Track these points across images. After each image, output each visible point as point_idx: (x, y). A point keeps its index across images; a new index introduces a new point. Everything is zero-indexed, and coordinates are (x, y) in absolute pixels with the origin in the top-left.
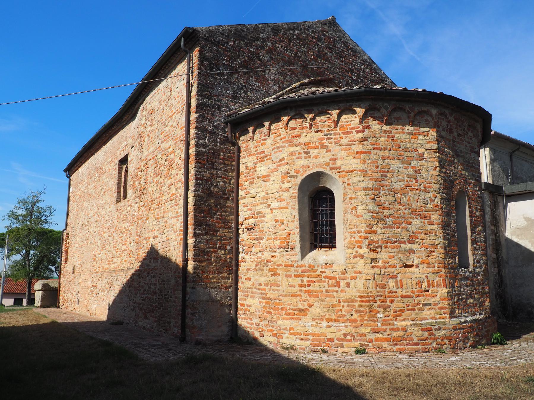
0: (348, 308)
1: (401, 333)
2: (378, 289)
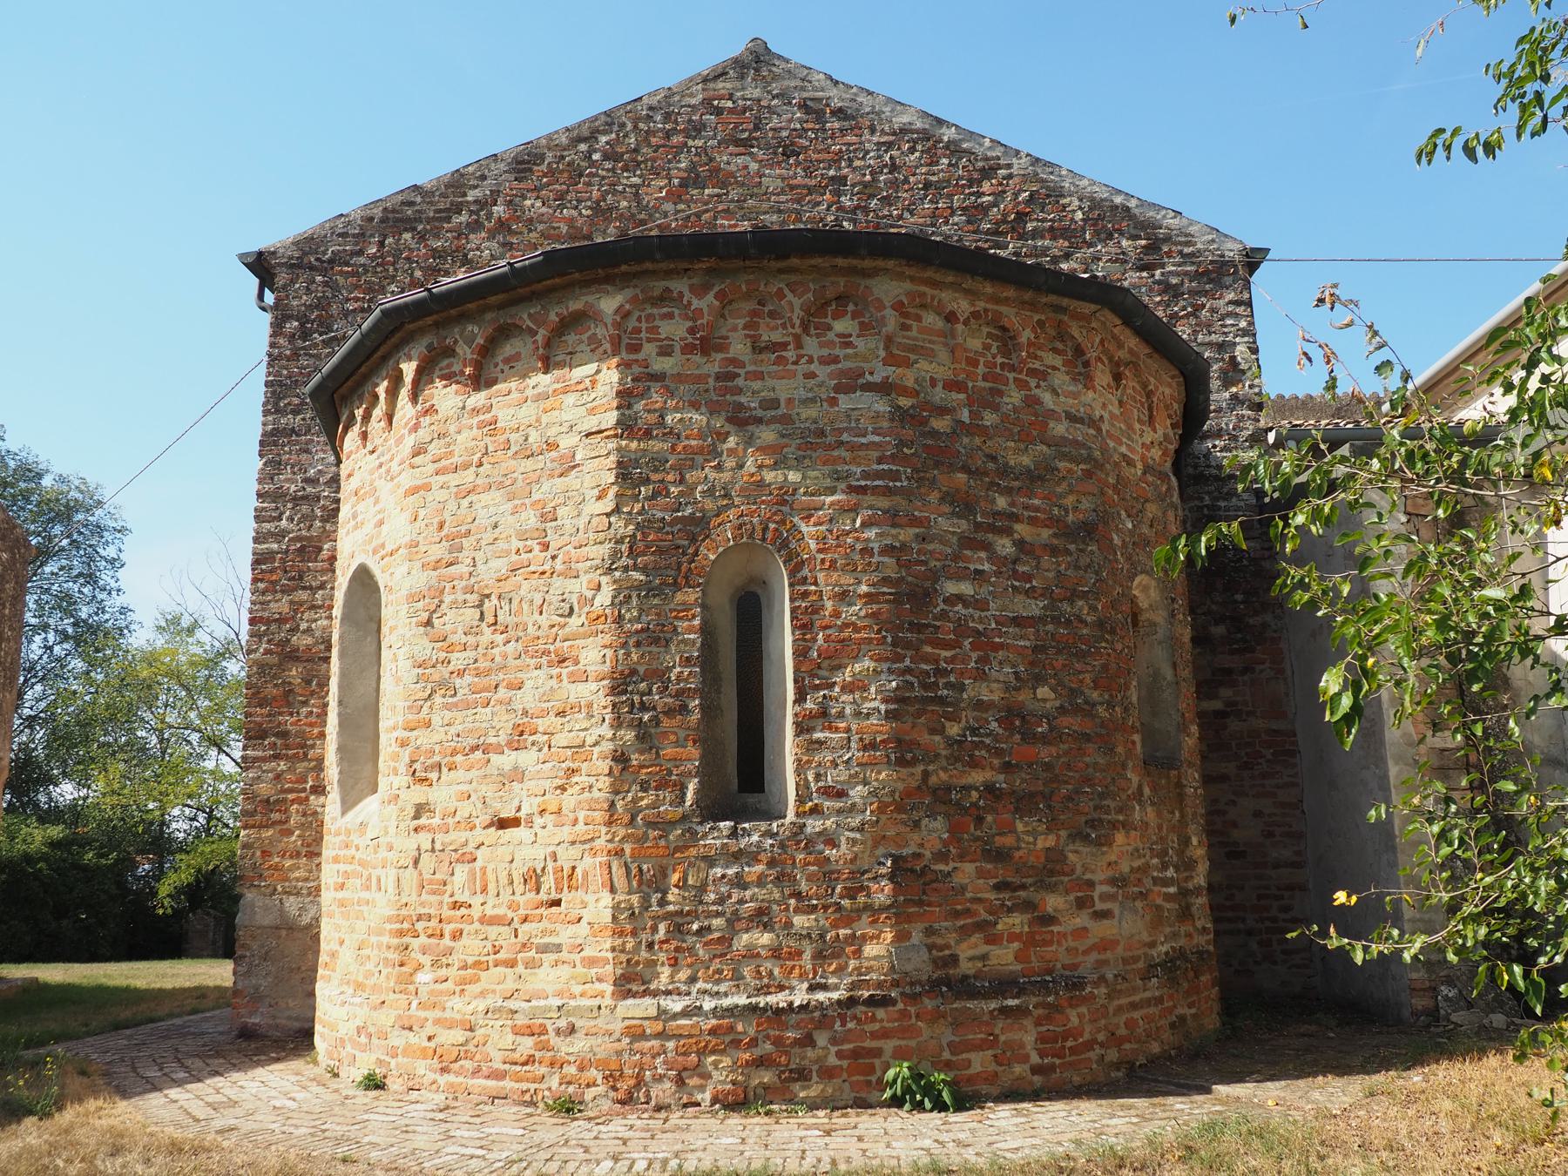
1: (458, 1036)
2: (425, 896)
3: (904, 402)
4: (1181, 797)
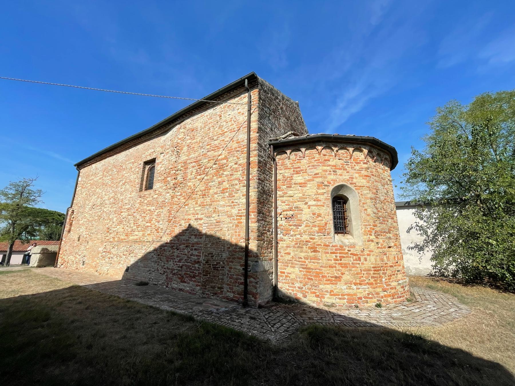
0: (367, 275)
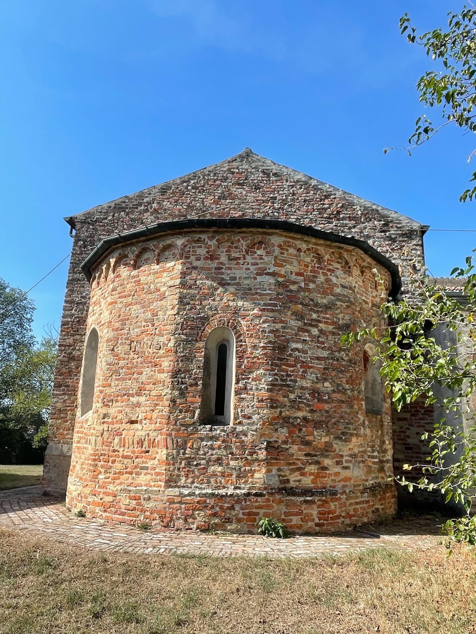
1: (110, 499)
2: (104, 447)
3: (280, 279)
4: (382, 426)
